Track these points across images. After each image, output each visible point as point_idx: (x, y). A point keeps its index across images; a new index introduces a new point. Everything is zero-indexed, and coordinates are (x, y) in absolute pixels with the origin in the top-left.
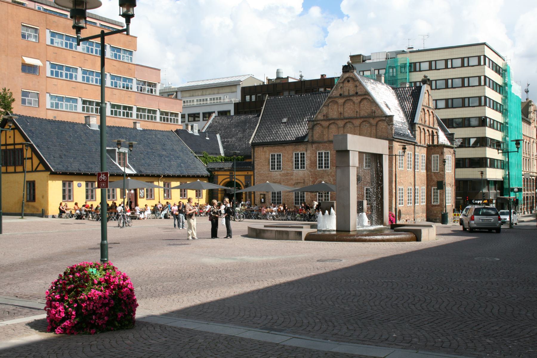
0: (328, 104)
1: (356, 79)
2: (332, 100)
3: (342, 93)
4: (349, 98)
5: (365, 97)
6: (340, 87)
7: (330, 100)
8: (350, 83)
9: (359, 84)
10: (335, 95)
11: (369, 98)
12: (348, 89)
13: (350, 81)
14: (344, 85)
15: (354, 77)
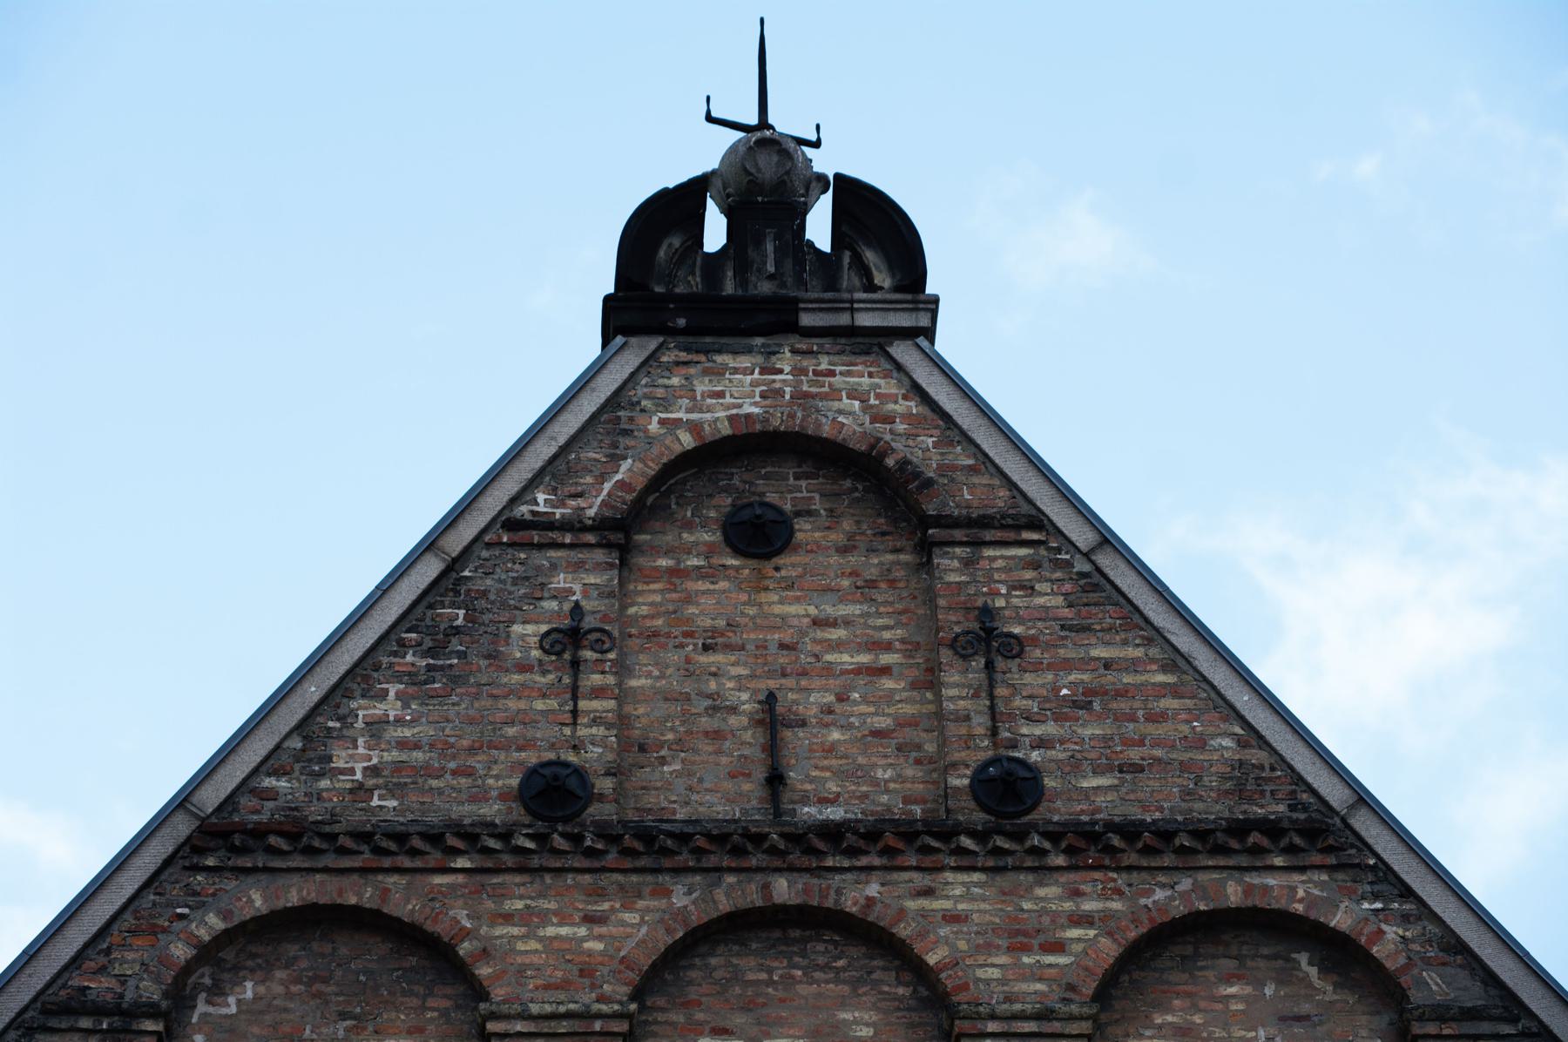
0: (180, 997)
1: (970, 495)
2: (295, 893)
3: (594, 756)
4: (784, 889)
5: (1233, 894)
6: (527, 632)
7: (257, 900)
8: (790, 563)
9: (1049, 599)
10: (392, 778)
11: (1340, 920)
12: (746, 702)
13: (805, 531)
14: (647, 601)
15: (925, 450)
